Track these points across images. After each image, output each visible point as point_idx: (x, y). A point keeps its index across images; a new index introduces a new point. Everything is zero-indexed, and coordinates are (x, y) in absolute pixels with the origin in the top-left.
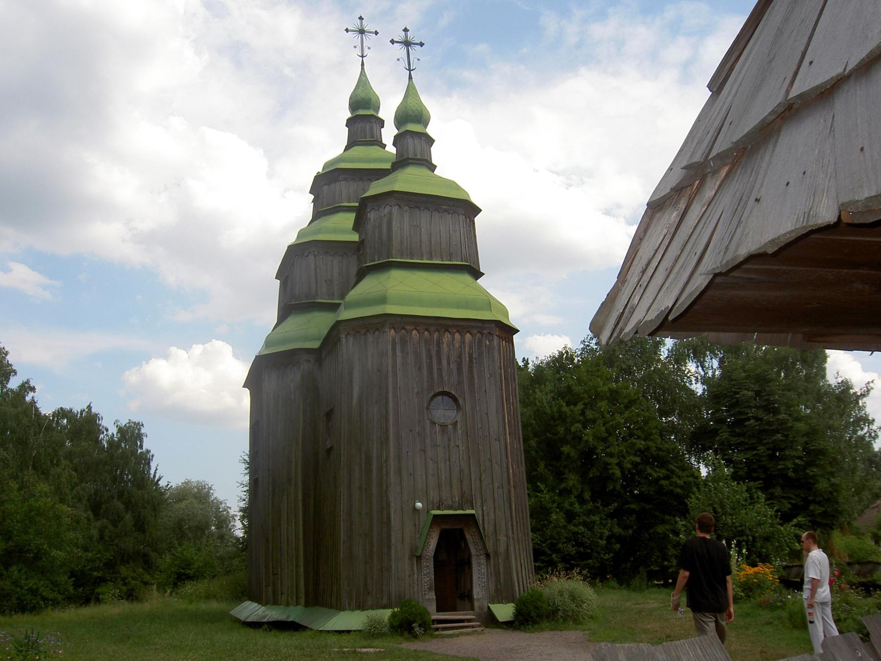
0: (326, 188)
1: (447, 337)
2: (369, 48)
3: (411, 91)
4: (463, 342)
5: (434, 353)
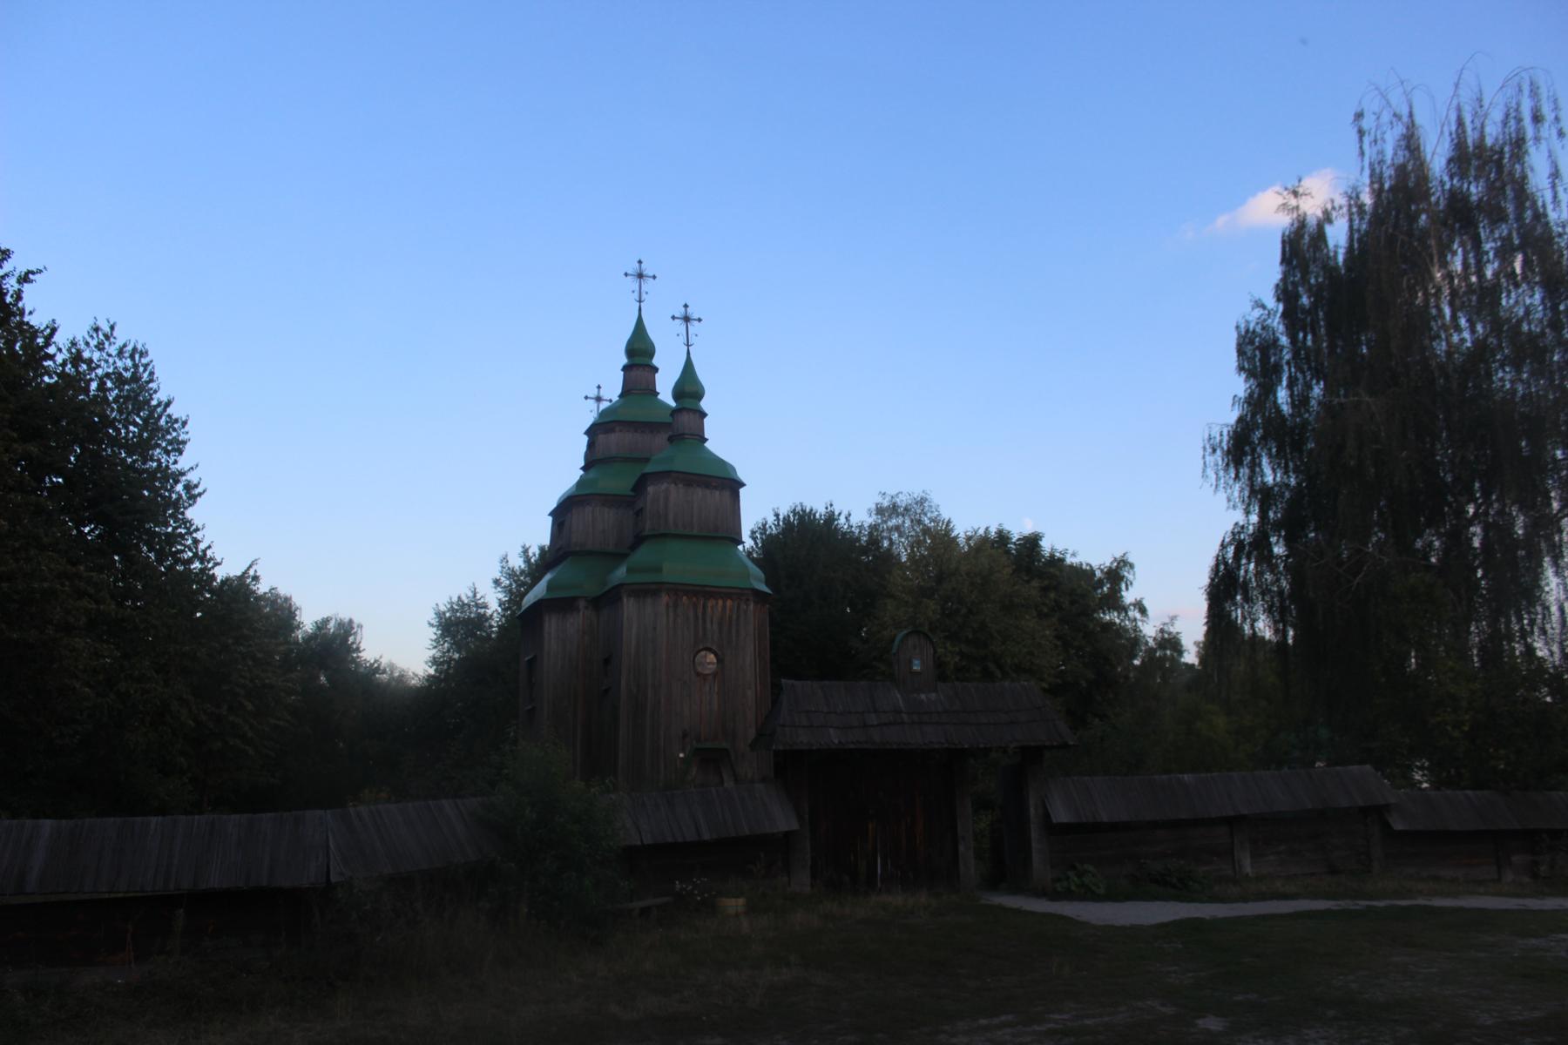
1: (711, 603)
2: (647, 293)
4: (724, 607)
5: (700, 615)
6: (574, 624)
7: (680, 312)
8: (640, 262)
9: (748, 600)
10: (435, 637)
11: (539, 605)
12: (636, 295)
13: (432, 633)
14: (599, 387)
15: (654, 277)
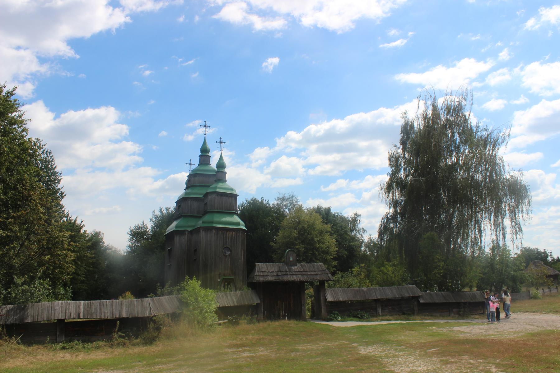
0: (193, 178)
3: (221, 158)
5: (225, 237)
6: (184, 239)
7: (219, 140)
10: (130, 238)
11: (173, 233)
13: (129, 237)
14: (190, 160)
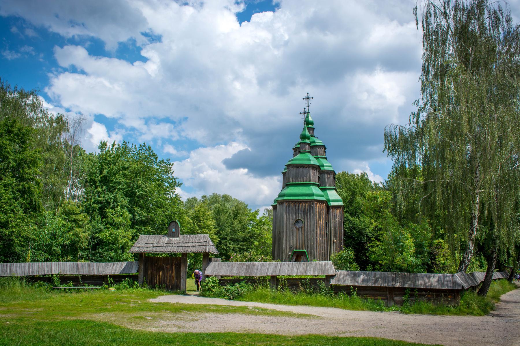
4: (305, 206)
5: (297, 209)
8: (308, 94)
9: (313, 203)
12: (307, 105)
15: (313, 98)
